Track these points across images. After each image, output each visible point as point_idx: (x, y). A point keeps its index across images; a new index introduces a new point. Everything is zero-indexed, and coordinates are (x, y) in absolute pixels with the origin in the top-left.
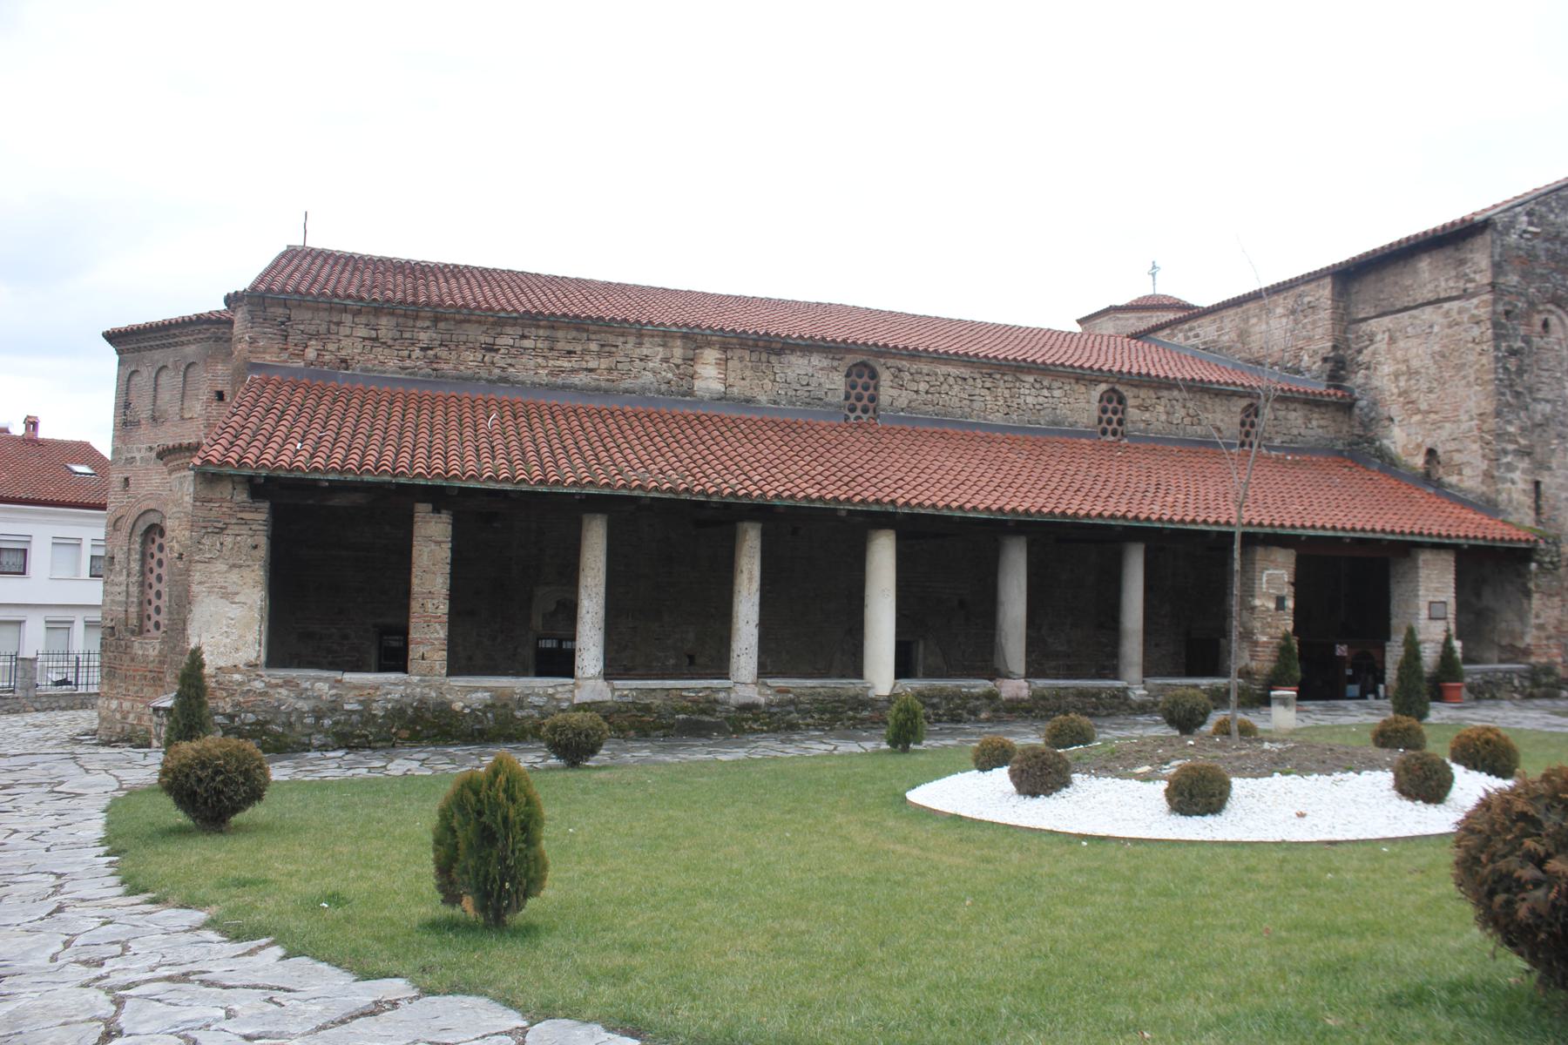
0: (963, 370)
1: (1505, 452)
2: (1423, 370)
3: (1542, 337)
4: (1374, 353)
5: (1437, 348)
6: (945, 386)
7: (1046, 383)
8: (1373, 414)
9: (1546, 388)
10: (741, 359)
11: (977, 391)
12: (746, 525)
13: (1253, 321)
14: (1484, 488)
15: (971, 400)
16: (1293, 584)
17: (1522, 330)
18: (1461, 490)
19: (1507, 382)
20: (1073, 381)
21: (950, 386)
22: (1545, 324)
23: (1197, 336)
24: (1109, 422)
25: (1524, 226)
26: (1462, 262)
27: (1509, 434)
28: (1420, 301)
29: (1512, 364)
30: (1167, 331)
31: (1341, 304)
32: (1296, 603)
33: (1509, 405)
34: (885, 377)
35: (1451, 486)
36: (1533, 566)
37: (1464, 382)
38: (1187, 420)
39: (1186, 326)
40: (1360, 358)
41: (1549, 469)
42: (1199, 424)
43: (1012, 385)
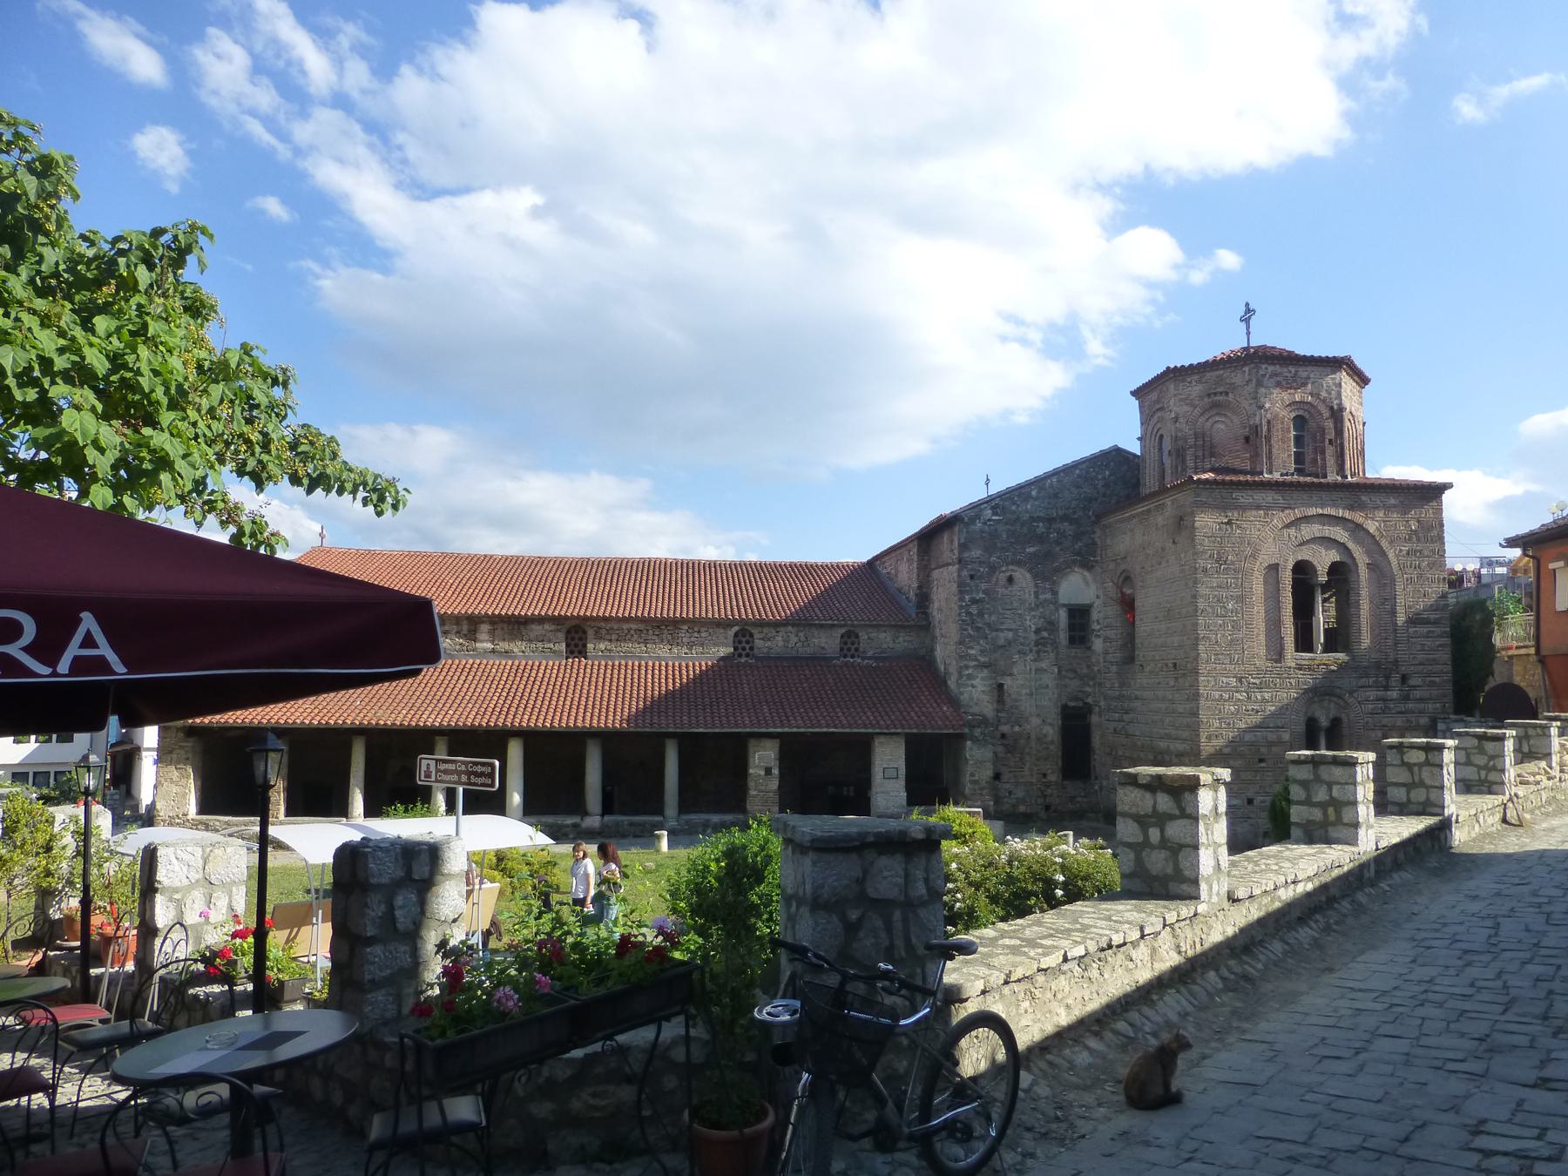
1: (967, 667)
3: (1006, 588)
6: (629, 636)
7: (696, 629)
10: (503, 629)
12: (437, 738)
17: (983, 586)
19: (969, 622)
22: (1010, 580)
24: (744, 649)
27: (970, 655)
29: (974, 610)
31: (926, 558)
34: (591, 633)
36: (969, 743)
41: (1011, 675)
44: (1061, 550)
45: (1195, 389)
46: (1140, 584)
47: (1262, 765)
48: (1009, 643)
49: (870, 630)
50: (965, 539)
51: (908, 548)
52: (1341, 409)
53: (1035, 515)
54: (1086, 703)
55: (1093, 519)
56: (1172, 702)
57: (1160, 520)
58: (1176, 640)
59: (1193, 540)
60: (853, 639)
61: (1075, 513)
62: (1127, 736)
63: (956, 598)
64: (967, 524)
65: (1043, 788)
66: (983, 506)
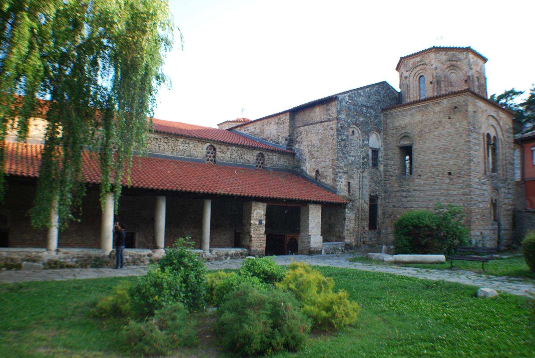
0: (156, 135)
1: (339, 172)
2: (316, 144)
4: (301, 138)
5: (320, 137)
6: (150, 141)
8: (300, 158)
9: (353, 152)
11: (161, 144)
13: (265, 126)
14: (333, 184)
15: (159, 147)
16: (265, 215)
18: (326, 184)
19: (340, 150)
20: (197, 142)
21: (152, 141)
22: (353, 132)
23: (248, 130)
24: (210, 157)
25: (347, 100)
26: (329, 110)
27: (341, 166)
28: (316, 122)
30: (239, 128)
31: (292, 122)
32: (266, 222)
33: (341, 157)
35: (323, 183)
36: (347, 210)
37: (328, 149)
38: (238, 157)
39: (245, 127)
40: (297, 140)
42: (242, 159)
43: (174, 142)
44: (371, 122)
45: (443, 57)
46: (419, 138)
47: (484, 218)
48: (353, 162)
49: (269, 154)
50: (340, 108)
51: (279, 117)
52: (486, 79)
53: (363, 104)
54: (376, 194)
55: (380, 110)
56: (447, 190)
57: (437, 109)
58: (451, 162)
59: (467, 116)
60: (261, 157)
61: (375, 106)
62: (405, 208)
63: (335, 137)
64: (340, 102)
65: (363, 234)
66: (346, 95)
